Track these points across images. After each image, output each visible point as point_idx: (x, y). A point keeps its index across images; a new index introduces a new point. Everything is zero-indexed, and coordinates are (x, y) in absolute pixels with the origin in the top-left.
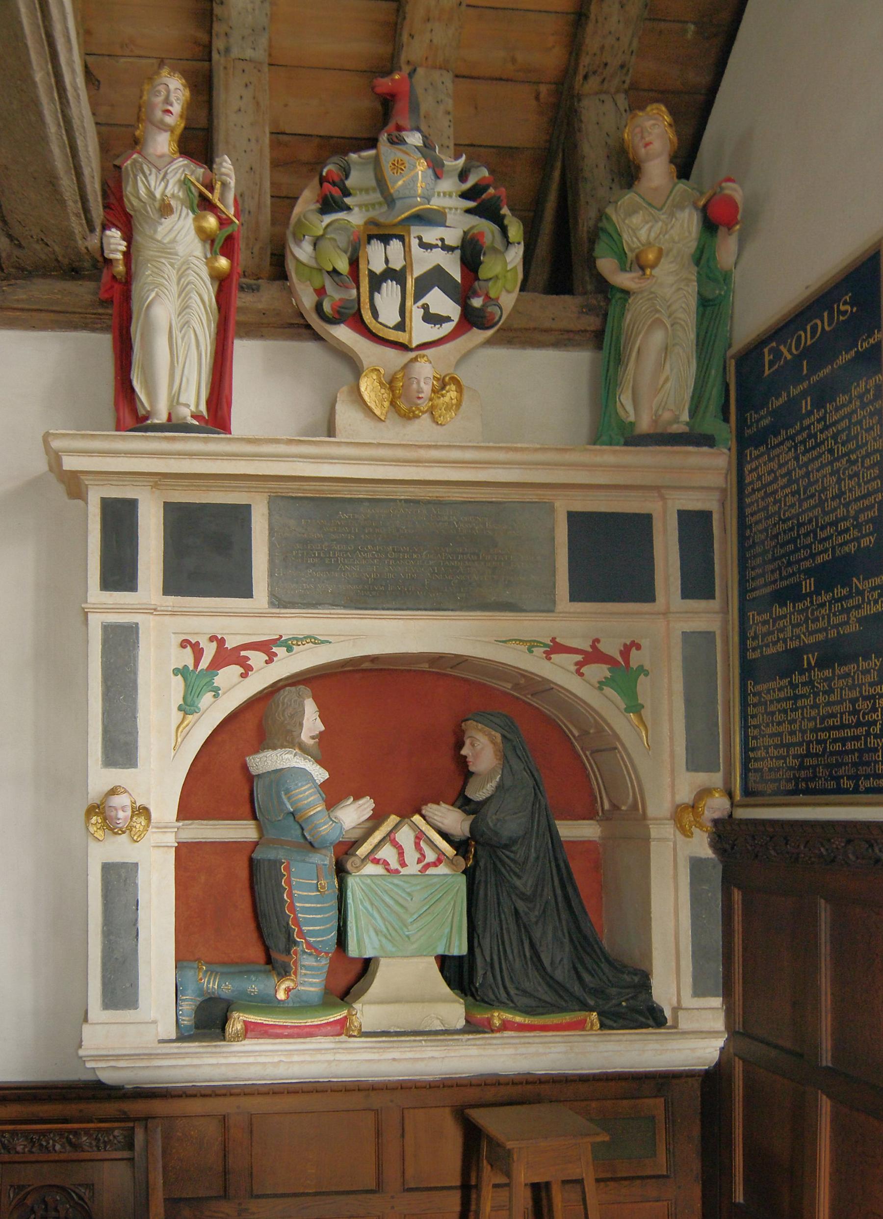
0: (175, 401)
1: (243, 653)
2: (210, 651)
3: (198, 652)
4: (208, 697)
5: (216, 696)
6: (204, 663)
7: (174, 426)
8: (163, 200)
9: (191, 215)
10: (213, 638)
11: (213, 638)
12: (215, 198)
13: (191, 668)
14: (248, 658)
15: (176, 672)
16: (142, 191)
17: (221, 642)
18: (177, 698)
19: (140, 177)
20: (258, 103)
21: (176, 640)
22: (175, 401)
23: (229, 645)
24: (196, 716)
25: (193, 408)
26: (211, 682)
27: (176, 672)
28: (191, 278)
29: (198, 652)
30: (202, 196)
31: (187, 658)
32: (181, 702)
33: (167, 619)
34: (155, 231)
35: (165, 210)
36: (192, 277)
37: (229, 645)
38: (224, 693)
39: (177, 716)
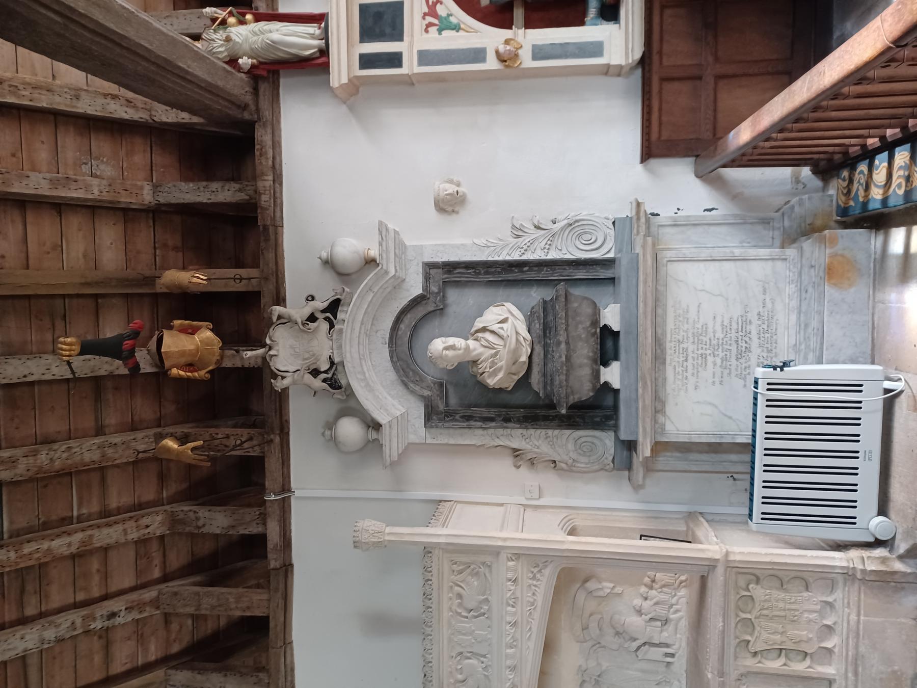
0: (312, 36)
1: (430, 3)
2: (430, 19)
3: (430, 25)
4: (453, 20)
5: (451, 15)
6: (436, 21)
7: (326, 37)
8: (224, 41)
9: (229, 28)
10: (424, 18)
11: (424, 18)
12: (221, 17)
13: (438, 27)
14: (433, 2)
15: (440, 33)
16: (220, 49)
17: (425, 14)
18: (452, 33)
19: (214, 50)
20: (167, 16)
21: (425, 35)
22: (312, 36)
23: (426, 10)
24: (461, 23)
25: (316, 29)
26: (445, 18)
27: (440, 33)
28: (257, 30)
29: (430, 25)
30: (219, 25)
31: (433, 30)
32: (454, 31)
33: (415, 38)
34: (238, 43)
35: (228, 39)
36: (256, 29)
37: (426, 10)
38: (450, 11)
39: (461, 33)
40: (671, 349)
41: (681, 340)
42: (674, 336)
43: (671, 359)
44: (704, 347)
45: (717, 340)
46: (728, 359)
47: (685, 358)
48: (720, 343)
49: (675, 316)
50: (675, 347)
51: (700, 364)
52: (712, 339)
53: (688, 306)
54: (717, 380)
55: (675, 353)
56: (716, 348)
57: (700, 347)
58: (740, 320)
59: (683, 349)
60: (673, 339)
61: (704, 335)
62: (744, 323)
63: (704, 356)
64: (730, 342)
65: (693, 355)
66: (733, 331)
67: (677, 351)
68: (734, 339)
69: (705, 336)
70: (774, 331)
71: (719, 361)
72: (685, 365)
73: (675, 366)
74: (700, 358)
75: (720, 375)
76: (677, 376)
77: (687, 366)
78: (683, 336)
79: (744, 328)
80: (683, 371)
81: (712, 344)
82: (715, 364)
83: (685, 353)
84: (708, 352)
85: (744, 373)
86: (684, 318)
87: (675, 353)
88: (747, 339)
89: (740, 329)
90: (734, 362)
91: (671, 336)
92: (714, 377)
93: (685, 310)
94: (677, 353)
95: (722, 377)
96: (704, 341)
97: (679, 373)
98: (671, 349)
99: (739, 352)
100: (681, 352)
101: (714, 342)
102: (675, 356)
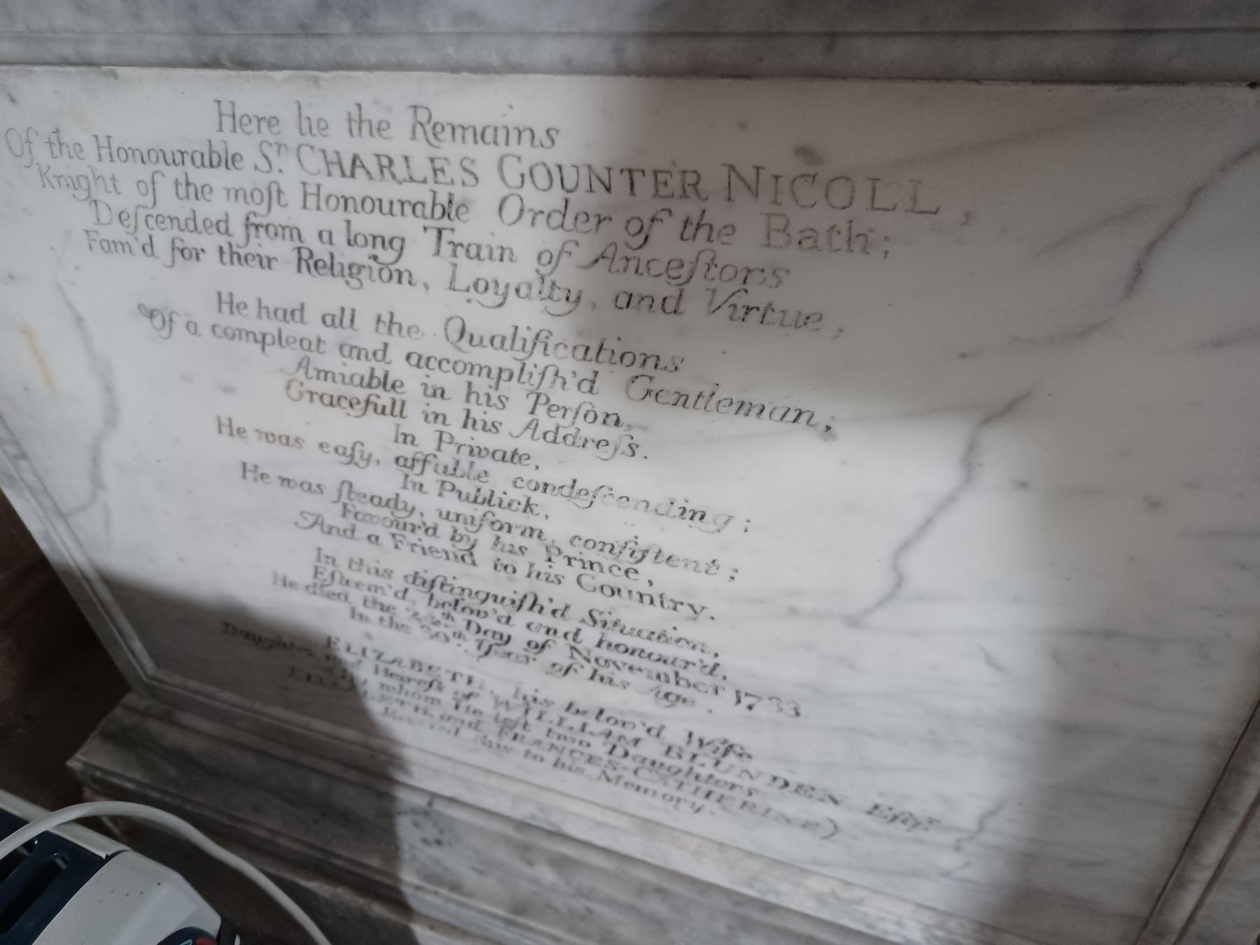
40: (357, 123)
41: (464, 231)
42: (485, 156)
43: (273, 121)
44: (454, 409)
45: (519, 495)
46: (412, 538)
47: (321, 252)
48: (503, 515)
49: (692, 187)
50: (386, 165)
51: (319, 361)
52: (526, 472)
53: (806, 320)
54: (256, 451)
55: (333, 163)
56: (466, 486)
57: (438, 378)
58: (685, 653)
59: (396, 244)
60: (452, 150)
61: (546, 423)
62: (668, 670)
63: (385, 398)
64: (523, 570)
65: (365, 321)
66: (600, 602)
67: (357, 187)
68: (545, 591)
69: (532, 426)
70: (629, 777)
71: (383, 481)
72: (265, 245)
73: (231, 161)
74: (361, 368)
75: (295, 474)
76: (174, 172)
77: (267, 263)
78: (504, 254)
79: (634, 660)
80: (221, 225)
81: (482, 464)
82: (352, 455)
83: (360, 255)
84: (426, 438)
85: (356, 597)
86: (674, 268)
87: (333, 163)
88: (559, 652)
89: (614, 637)
90: (404, 563)
91: (480, 136)
92: (269, 437)
93: (758, 295)
94: (337, 185)
95: (285, 481)
96: (493, 415)
97: (201, 192)
98: (357, 123)
99: (474, 603)
100: (368, 223)
101: (500, 477)
102: (314, 162)
